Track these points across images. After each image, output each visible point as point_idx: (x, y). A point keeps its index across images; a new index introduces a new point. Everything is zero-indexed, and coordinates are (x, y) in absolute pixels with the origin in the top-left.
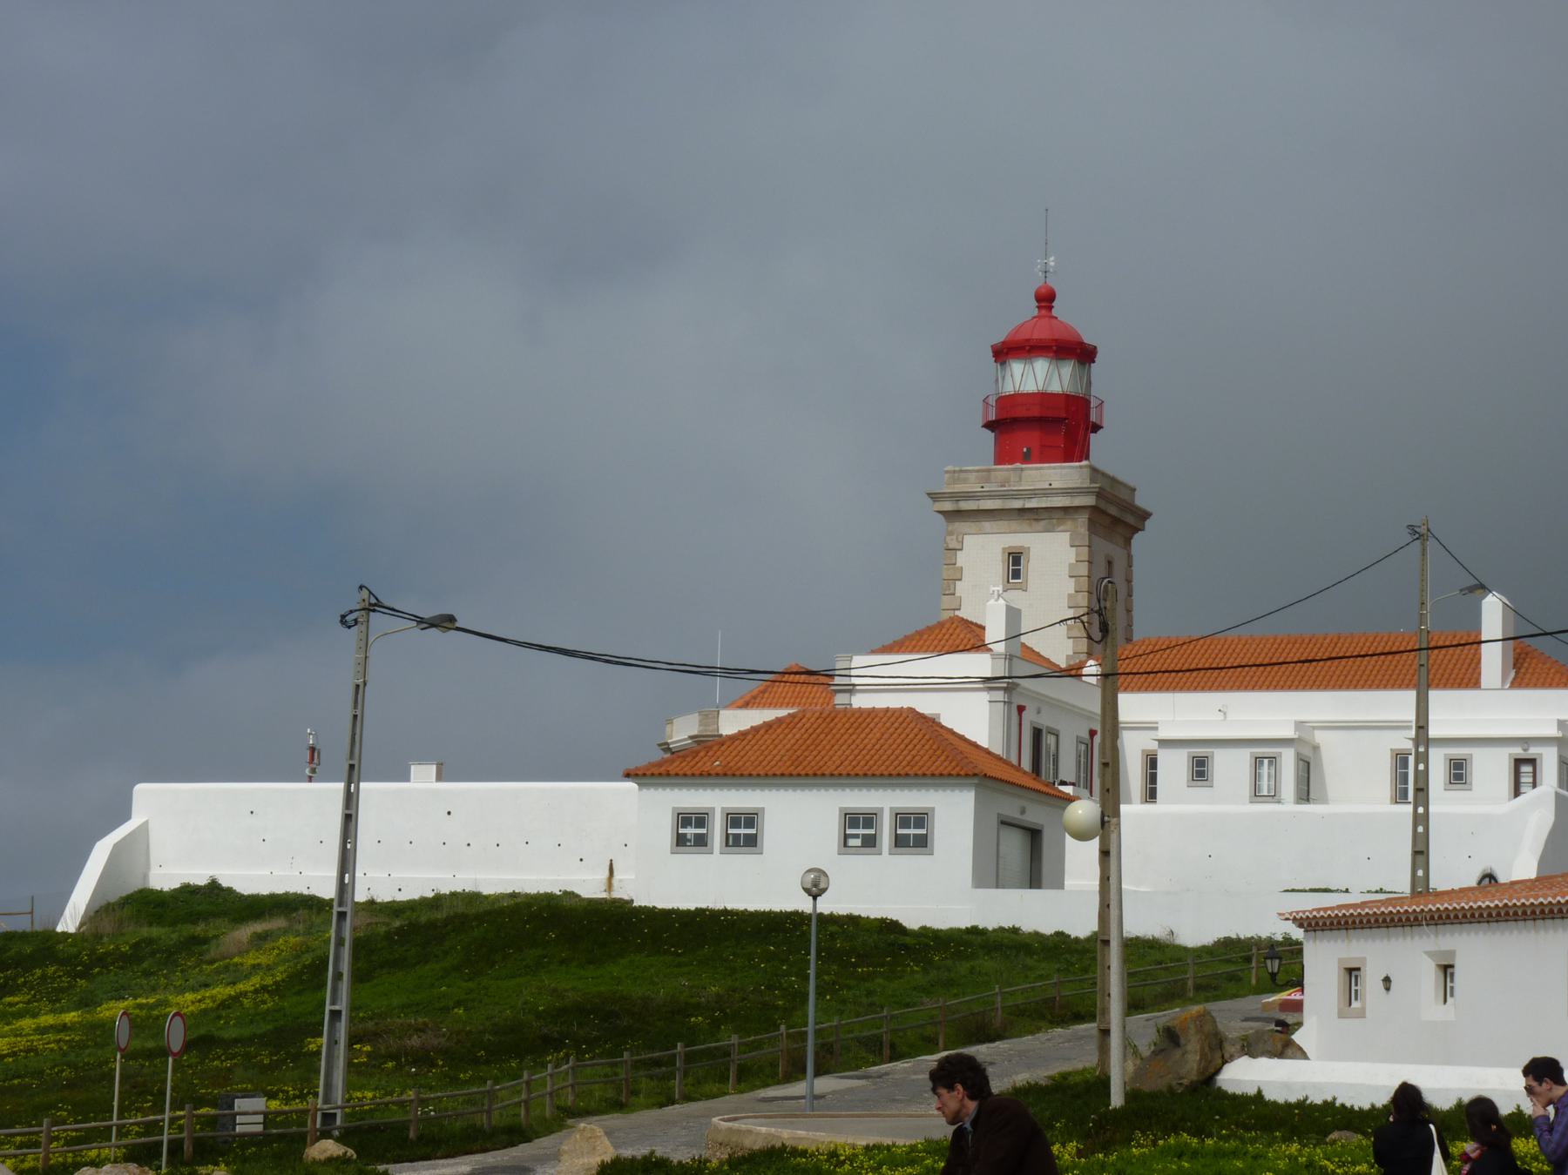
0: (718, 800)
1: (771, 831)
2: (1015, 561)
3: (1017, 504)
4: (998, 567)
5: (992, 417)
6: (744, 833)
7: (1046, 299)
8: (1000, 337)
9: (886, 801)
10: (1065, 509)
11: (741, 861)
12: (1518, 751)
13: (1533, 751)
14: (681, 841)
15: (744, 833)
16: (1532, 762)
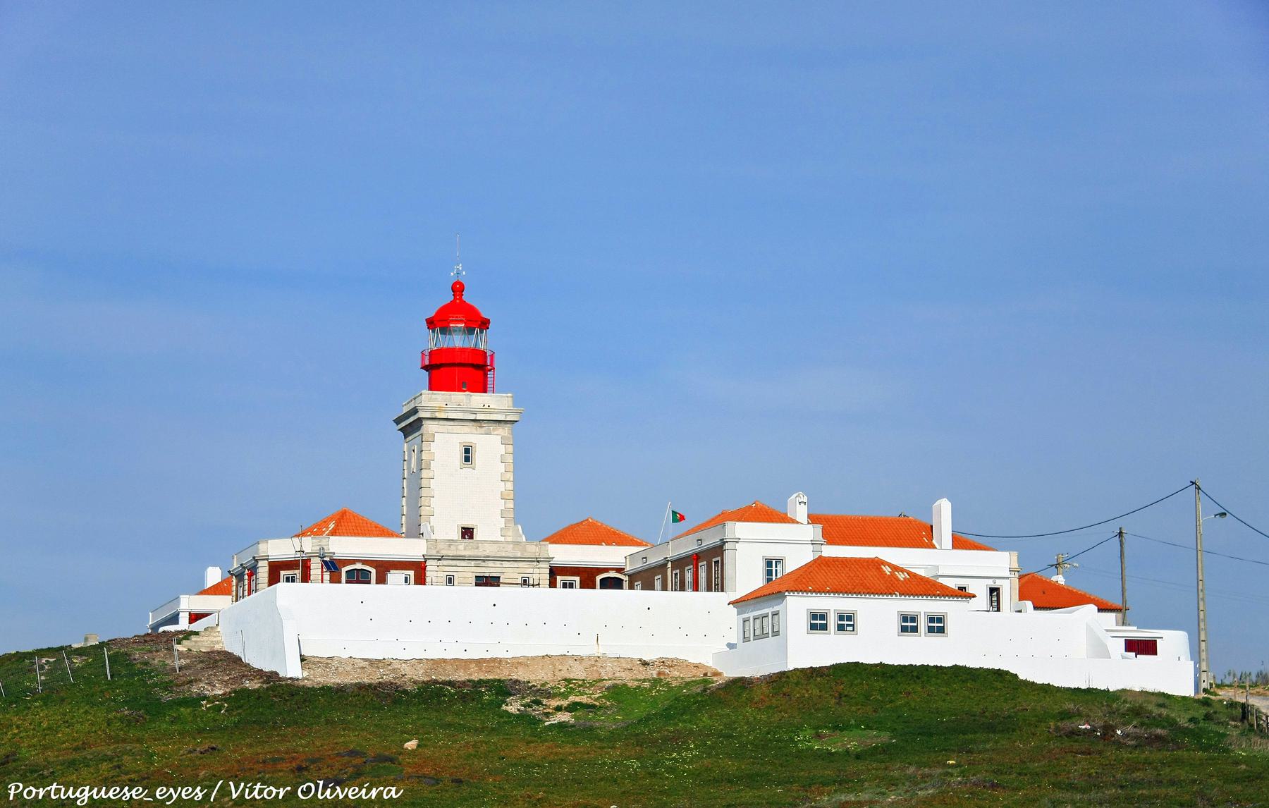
0: (832, 604)
1: (860, 621)
2: (467, 450)
3: (473, 417)
4: (459, 454)
5: (427, 363)
6: (846, 622)
7: (458, 288)
8: (431, 314)
9: (922, 607)
10: (506, 422)
11: (844, 638)
12: (991, 583)
13: (998, 583)
14: (813, 627)
15: (846, 622)
16: (997, 590)
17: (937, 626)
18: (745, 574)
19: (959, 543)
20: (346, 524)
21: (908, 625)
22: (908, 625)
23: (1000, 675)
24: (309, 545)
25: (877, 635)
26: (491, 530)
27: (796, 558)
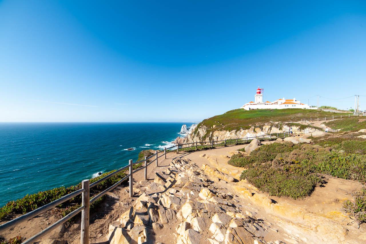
0: (287, 105)
1: (289, 106)
6: (288, 106)
9: (294, 105)
15: (288, 106)
17: (295, 106)
18: (279, 103)
19: (296, 101)
20: (251, 102)
21: (293, 106)
22: (293, 106)
23: (301, 109)
24: (250, 103)
25: (290, 106)
26: (261, 102)
27: (283, 102)
